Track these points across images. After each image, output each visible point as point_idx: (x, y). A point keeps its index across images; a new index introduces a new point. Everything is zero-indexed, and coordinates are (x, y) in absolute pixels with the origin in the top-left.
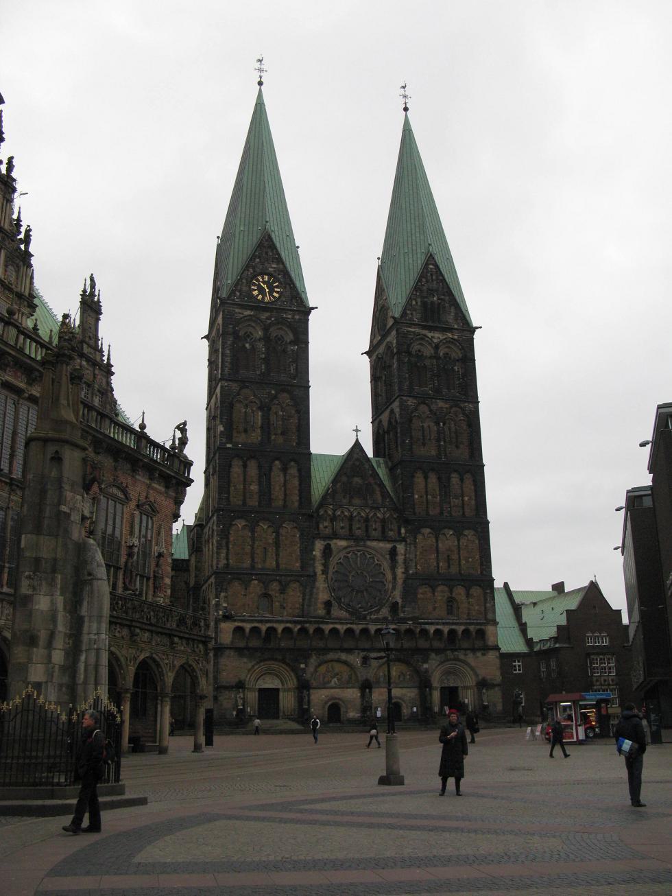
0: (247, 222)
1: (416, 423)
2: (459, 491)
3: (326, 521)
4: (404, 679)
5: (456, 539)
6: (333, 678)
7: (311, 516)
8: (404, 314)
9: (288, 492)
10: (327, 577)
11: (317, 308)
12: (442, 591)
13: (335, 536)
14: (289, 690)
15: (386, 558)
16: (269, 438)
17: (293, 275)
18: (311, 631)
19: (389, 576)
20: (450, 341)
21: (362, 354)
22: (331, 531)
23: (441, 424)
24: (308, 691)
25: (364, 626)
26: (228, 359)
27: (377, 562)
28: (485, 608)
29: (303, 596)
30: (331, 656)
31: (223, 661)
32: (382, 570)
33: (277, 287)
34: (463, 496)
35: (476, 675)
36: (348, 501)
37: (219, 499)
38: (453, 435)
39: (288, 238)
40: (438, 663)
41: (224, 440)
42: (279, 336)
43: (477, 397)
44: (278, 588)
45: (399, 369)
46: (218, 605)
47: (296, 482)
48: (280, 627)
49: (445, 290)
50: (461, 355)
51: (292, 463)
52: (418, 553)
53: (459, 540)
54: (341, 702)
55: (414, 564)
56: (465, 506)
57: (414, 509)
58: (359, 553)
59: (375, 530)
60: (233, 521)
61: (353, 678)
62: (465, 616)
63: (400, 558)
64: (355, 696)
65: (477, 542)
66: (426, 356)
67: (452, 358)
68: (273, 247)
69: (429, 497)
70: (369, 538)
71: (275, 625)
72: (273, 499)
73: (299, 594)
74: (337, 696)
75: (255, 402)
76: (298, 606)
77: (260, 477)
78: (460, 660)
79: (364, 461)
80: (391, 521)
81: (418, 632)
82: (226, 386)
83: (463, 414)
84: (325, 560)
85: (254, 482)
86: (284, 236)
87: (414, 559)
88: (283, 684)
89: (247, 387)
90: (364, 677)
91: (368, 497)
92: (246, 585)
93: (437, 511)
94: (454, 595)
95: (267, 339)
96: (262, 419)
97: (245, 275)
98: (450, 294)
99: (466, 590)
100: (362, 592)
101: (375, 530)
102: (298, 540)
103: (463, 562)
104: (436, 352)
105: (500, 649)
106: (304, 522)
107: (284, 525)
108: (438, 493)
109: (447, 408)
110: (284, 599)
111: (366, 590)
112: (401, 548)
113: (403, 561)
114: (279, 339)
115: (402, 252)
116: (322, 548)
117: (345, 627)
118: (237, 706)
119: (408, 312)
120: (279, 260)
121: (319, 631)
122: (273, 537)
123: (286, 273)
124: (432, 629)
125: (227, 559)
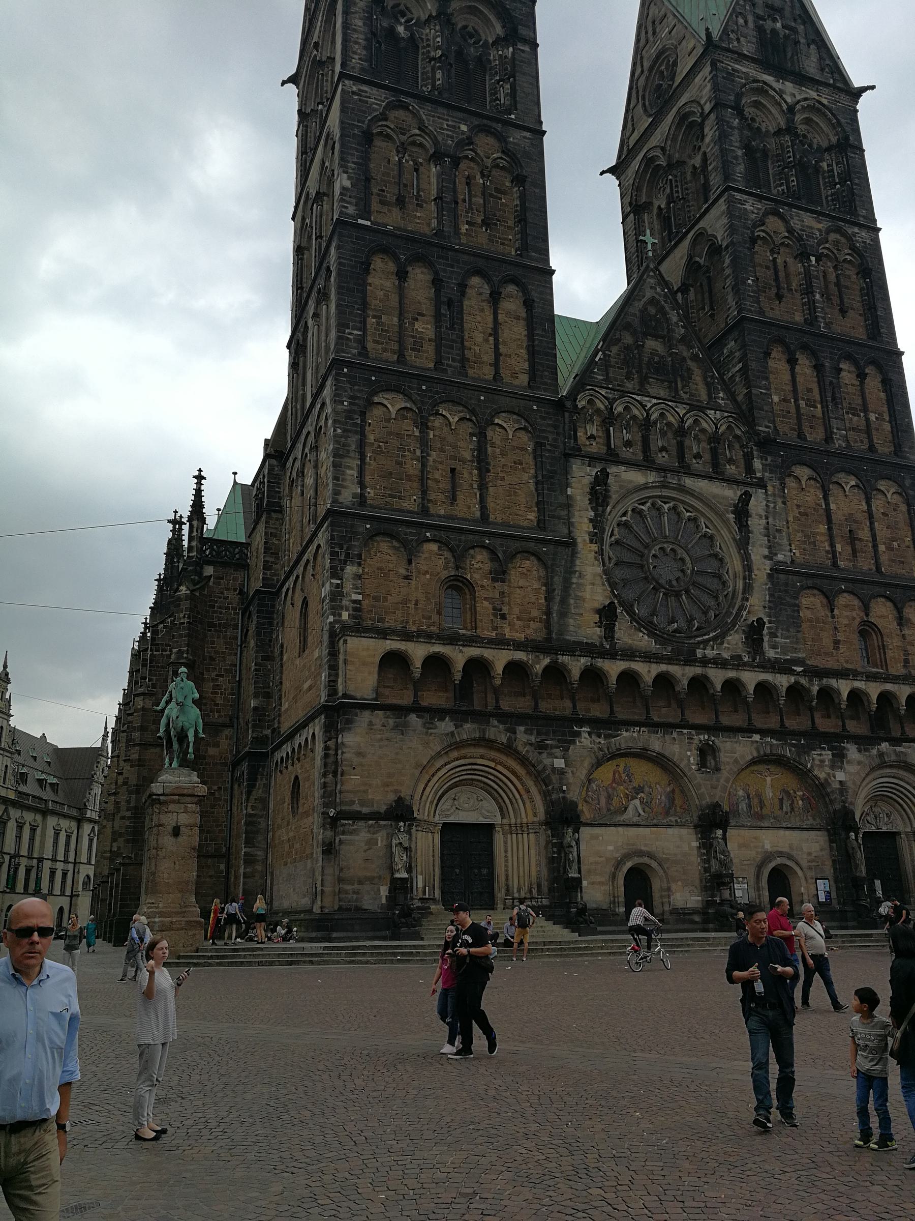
1: (763, 253)
2: (860, 401)
3: (591, 421)
4: (792, 809)
7: (559, 405)
8: (725, 32)
9: (502, 349)
12: (847, 606)
13: (612, 457)
14: (521, 828)
15: (728, 519)
18: (576, 673)
19: (735, 563)
20: (811, 108)
21: (602, 174)
22: (604, 449)
23: (813, 259)
24: (576, 830)
25: (698, 670)
29: (547, 591)
30: (627, 737)
31: (352, 739)
32: (718, 550)
34: (865, 410)
36: (637, 387)
37: (339, 338)
38: (833, 288)
41: (351, 210)
42: (470, 29)
43: (875, 221)
44: (487, 567)
45: (723, 137)
46: (337, 595)
48: (500, 659)
49: (798, 13)
50: (834, 140)
51: (511, 289)
54: (654, 864)
55: (785, 541)
56: (874, 433)
57: (774, 422)
58: (666, 507)
59: (698, 456)
60: (376, 393)
61: (678, 802)
63: (756, 524)
65: (904, 508)
66: (767, 131)
69: (802, 403)
71: (487, 653)
73: (536, 585)
74: (643, 848)
75: (421, 145)
76: (535, 613)
79: (667, 307)
82: (354, 93)
83: (850, 249)
85: (423, 315)
88: (503, 816)
89: (405, 107)
91: (680, 386)
92: (410, 552)
100: (678, 595)
101: (698, 456)
102: (529, 459)
103: (882, 548)
104: (790, 122)
107: (496, 421)
108: (818, 398)
109: (820, 230)
110: (502, 594)
111: (687, 592)
116: (587, 481)
118: (392, 871)
119: (731, 36)
121: (592, 676)
122: (472, 447)
124: (844, 687)
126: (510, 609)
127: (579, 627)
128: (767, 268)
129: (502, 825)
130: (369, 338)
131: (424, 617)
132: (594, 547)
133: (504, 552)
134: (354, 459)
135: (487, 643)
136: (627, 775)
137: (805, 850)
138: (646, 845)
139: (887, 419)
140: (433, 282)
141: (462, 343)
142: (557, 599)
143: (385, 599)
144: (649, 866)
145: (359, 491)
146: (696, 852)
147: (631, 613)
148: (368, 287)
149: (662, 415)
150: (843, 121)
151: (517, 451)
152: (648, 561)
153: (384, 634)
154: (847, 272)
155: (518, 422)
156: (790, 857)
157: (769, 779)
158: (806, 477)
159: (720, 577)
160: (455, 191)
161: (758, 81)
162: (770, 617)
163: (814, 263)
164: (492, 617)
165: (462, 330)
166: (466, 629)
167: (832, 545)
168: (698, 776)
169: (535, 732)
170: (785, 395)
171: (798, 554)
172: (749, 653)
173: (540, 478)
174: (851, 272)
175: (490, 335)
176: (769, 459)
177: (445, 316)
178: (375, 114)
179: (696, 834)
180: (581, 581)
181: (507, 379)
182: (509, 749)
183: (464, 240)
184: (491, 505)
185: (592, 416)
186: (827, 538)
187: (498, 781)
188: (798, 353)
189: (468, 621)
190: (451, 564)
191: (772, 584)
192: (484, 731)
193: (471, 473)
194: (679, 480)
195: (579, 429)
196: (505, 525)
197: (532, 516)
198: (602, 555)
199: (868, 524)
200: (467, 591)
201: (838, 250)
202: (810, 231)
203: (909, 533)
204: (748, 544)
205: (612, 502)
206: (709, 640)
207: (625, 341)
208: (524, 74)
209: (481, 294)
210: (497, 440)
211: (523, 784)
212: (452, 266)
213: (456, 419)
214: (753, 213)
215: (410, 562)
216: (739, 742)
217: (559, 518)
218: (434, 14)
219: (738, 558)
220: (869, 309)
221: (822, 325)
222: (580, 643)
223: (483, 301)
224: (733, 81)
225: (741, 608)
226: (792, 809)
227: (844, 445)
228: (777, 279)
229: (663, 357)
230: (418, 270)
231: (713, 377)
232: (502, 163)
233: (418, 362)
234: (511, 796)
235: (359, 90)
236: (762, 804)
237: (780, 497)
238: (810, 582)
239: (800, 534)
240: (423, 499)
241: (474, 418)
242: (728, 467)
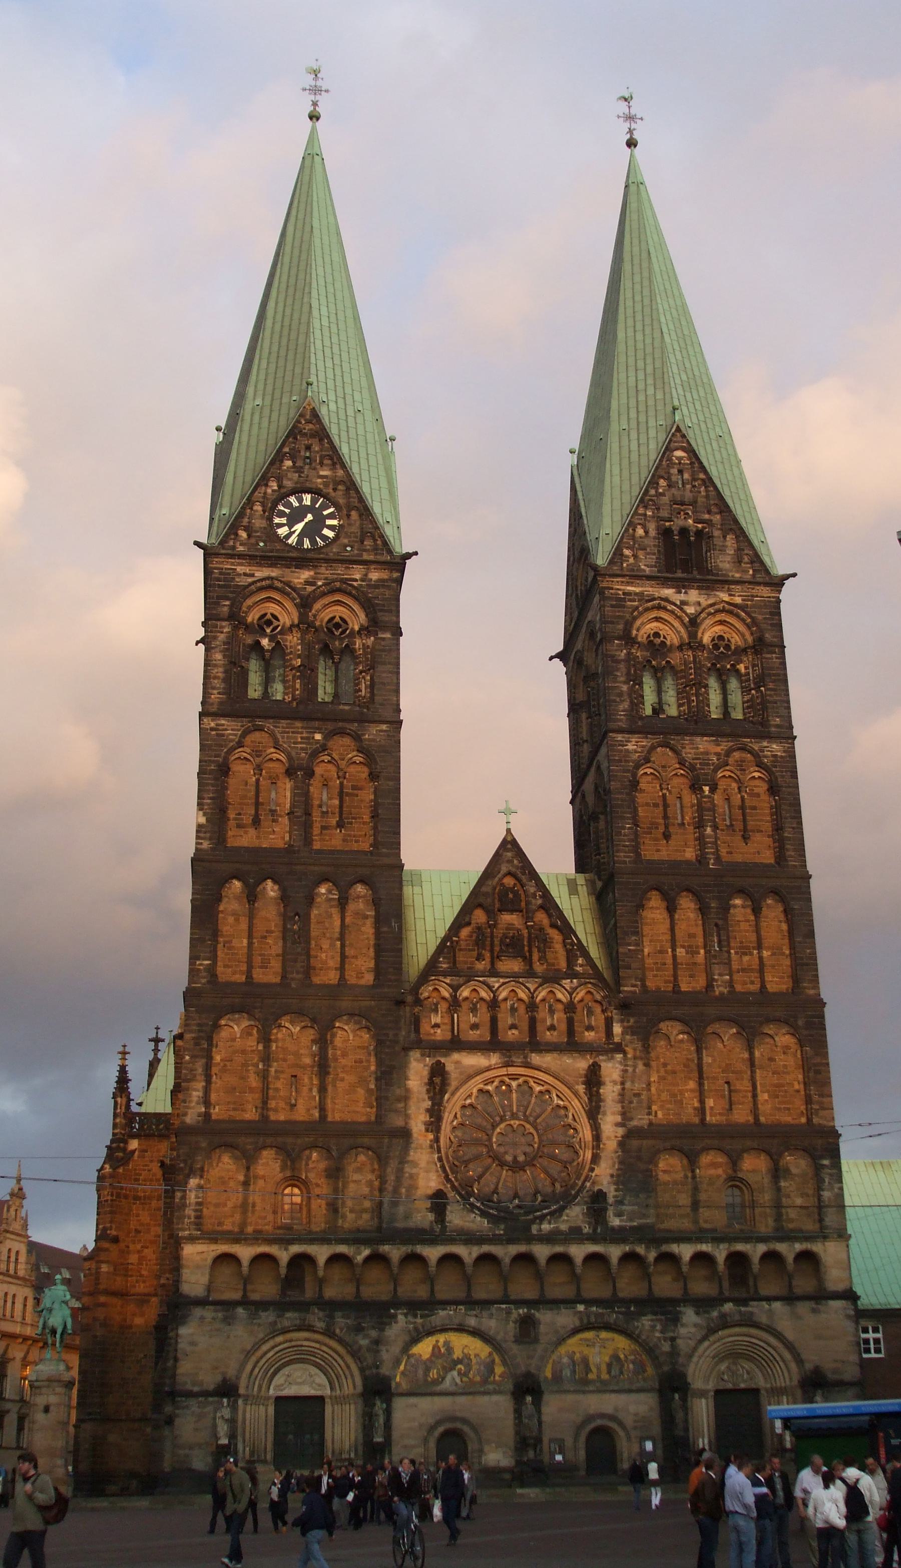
0: (269, 388)
1: (649, 789)
2: (753, 937)
3: (436, 1011)
8: (617, 555)
9: (349, 952)
10: (437, 1140)
11: (416, 553)
13: (456, 1044)
16: (308, 840)
17: (365, 489)
20: (723, 610)
22: (448, 1036)
23: (706, 789)
25: (522, 1248)
26: (219, 672)
27: (556, 1101)
30: (442, 1315)
33: (331, 516)
34: (759, 947)
35: (799, 1361)
36: (488, 967)
39: (359, 416)
40: (704, 1332)
43: (791, 727)
44: (322, 1165)
47: (368, 929)
48: (321, 1253)
49: (712, 502)
50: (750, 639)
51: (360, 889)
53: (750, 1049)
54: (466, 1429)
57: (643, 980)
58: (514, 1084)
59: (552, 1028)
61: (499, 1370)
62: (771, 1222)
63: (610, 1092)
67: (733, 648)
68: (322, 434)
69: (681, 952)
70: (535, 1045)
71: (310, 1249)
73: (370, 1176)
74: (458, 1414)
75: (278, 759)
78: (757, 1326)
79: (524, 878)
82: (212, 729)
83: (757, 766)
85: (272, 932)
86: (350, 412)
87: (645, 1093)
88: (332, 1389)
89: (260, 729)
90: (523, 1369)
92: (248, 1159)
93: (700, 983)
94: (740, 1175)
95: (305, 624)
96: (294, 795)
97: (258, 495)
98: (724, 508)
99: (771, 1158)
101: (552, 1028)
103: (763, 1097)
104: (693, 635)
105: (858, 1298)
107: (337, 1025)
108: (700, 940)
109: (716, 754)
112: (611, 1070)
113: (617, 1098)
114: (337, 626)
115: (614, 427)
116: (426, 1072)
117: (476, 1251)
119: (627, 552)
120: (335, 458)
123: (351, 486)
124: (686, 1251)
125: (207, 1102)
126: (343, 1203)
128: (656, 805)
129: (331, 1397)
130: (219, 964)
132: (431, 1136)
134: (200, 1081)
139: (787, 952)
142: (390, 1188)
143: (225, 1205)
145: (203, 1109)
148: (221, 915)
150: (760, 617)
153: (213, 1237)
154: (756, 790)
156: (612, 1418)
161: (654, 599)
162: (616, 1183)
163: (707, 793)
167: (702, 1102)
171: (660, 1114)
172: (589, 1224)
173: (379, 1074)
174: (761, 788)
175: (338, 939)
176: (632, 1020)
178: (232, 744)
180: (414, 1171)
182: (329, 1333)
183: (317, 846)
184: (329, 1105)
185: (436, 1005)
186: (697, 1094)
196: (343, 1123)
199: (749, 1073)
201: (741, 770)
202: (706, 757)
204: (598, 1113)
205: (451, 1089)
206: (547, 1215)
207: (479, 921)
208: (384, 663)
211: (344, 1361)
213: (298, 1028)
214: (636, 752)
217: (396, 1111)
218: (296, 622)
219: (589, 1128)
220: (777, 830)
221: (712, 861)
222: (407, 1230)
223: (331, 907)
224: (624, 606)
225: (587, 1178)
226: (621, 1373)
227: (726, 991)
228: (666, 817)
229: (518, 930)
231: (572, 944)
232: (358, 759)
235: (217, 725)
236: (588, 1369)
237: (641, 1059)
238: (668, 1145)
240: (263, 1108)
242: (586, 1034)
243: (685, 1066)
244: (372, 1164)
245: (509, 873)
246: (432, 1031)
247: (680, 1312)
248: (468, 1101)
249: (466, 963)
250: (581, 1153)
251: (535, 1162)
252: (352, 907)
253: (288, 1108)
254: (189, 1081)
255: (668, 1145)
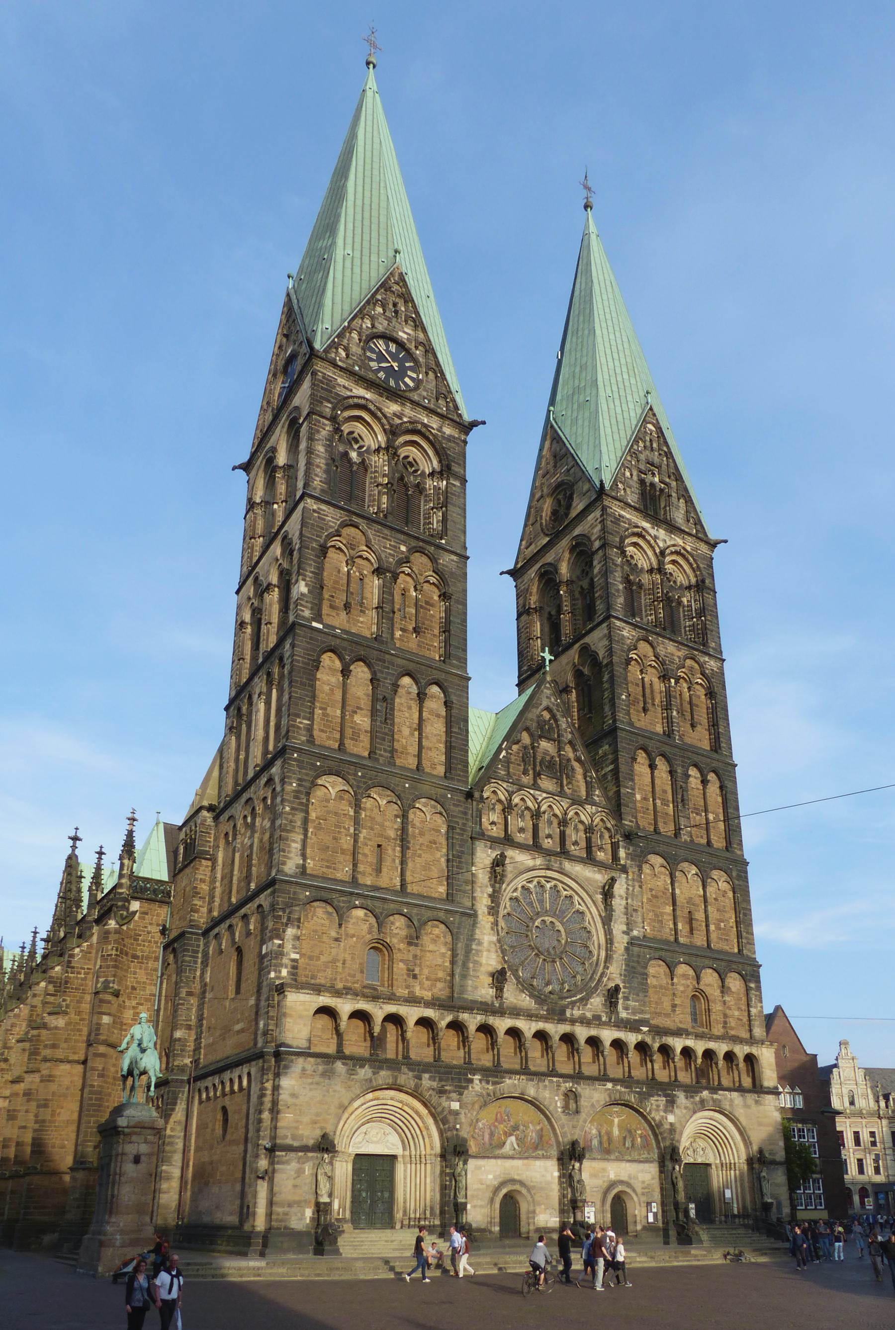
4: (633, 1145)
5: (700, 883)
6: (508, 1134)
7: (469, 795)
9: (425, 743)
10: (496, 923)
12: (685, 976)
13: (508, 840)
19: (599, 936)
28: (749, 1015)
30: (510, 1084)
36: (532, 782)
44: (404, 933)
51: (435, 689)
52: (645, 900)
55: (640, 920)
57: (636, 818)
58: (548, 886)
59: (576, 843)
63: (618, 903)
64: (549, 1178)
65: (730, 894)
69: (658, 802)
70: (564, 853)
72: (397, 751)
73: (443, 950)
74: (516, 1177)
76: (441, 974)
77: (374, 700)
80: (602, 832)
81: (656, 1049)
84: (493, 886)
85: (361, 709)
90: (569, 1138)
91: (565, 782)
92: (341, 918)
94: (702, 988)
101: (576, 843)
103: (712, 927)
106: (454, 805)
107: (417, 805)
110: (415, 956)
113: (623, 910)
116: (488, 861)
126: (421, 970)
127: (476, 988)
131: (349, 975)
132: (491, 919)
133: (419, 920)
135: (404, 1001)
136: (507, 1116)
137: (640, 1179)
138: (518, 1174)
140: (371, 680)
141: (393, 736)
142: (460, 963)
144: (519, 1192)
146: (556, 1181)
147: (517, 978)
149: (550, 806)
151: (433, 832)
152: (531, 931)
155: (435, 807)
156: (628, 1185)
157: (616, 1120)
158: (658, 865)
159: (587, 947)
160: (393, 602)
164: (405, 977)
165: (393, 725)
166: (383, 986)
167: (675, 924)
168: (563, 1117)
169: (437, 1079)
170: (646, 795)
173: (451, 857)
175: (415, 730)
176: (631, 849)
177: (380, 711)
179: (559, 1165)
180: (479, 948)
181: (428, 770)
182: (415, 1094)
184: (409, 878)
185: (494, 805)
187: (403, 1119)
188: (657, 759)
189: (386, 979)
190: (375, 929)
191: (628, 955)
192: (396, 1078)
193: (394, 850)
194: (561, 864)
195: (483, 816)
196: (420, 896)
197: (442, 889)
198: (497, 925)
200: (386, 952)
203: (734, 916)
204: (611, 920)
205: (507, 880)
207: (523, 741)
209: (410, 693)
210: (417, 822)
212: (388, 668)
213: (385, 802)
215: (340, 925)
216: (595, 1089)
217: (465, 892)
223: (411, 699)
230: (359, 670)
232: (432, 580)
233: (355, 751)
234: (413, 1132)
236: (610, 1140)
239: (651, 914)
240: (354, 871)
241: (399, 802)
243: (664, 893)
244: (445, 937)
245: (547, 709)
246: (490, 828)
247: (675, 1095)
248: (515, 894)
249: (515, 774)
250: (595, 953)
251: (564, 956)
252: (430, 704)
253: (374, 874)
254: (288, 831)
255: (657, 955)
